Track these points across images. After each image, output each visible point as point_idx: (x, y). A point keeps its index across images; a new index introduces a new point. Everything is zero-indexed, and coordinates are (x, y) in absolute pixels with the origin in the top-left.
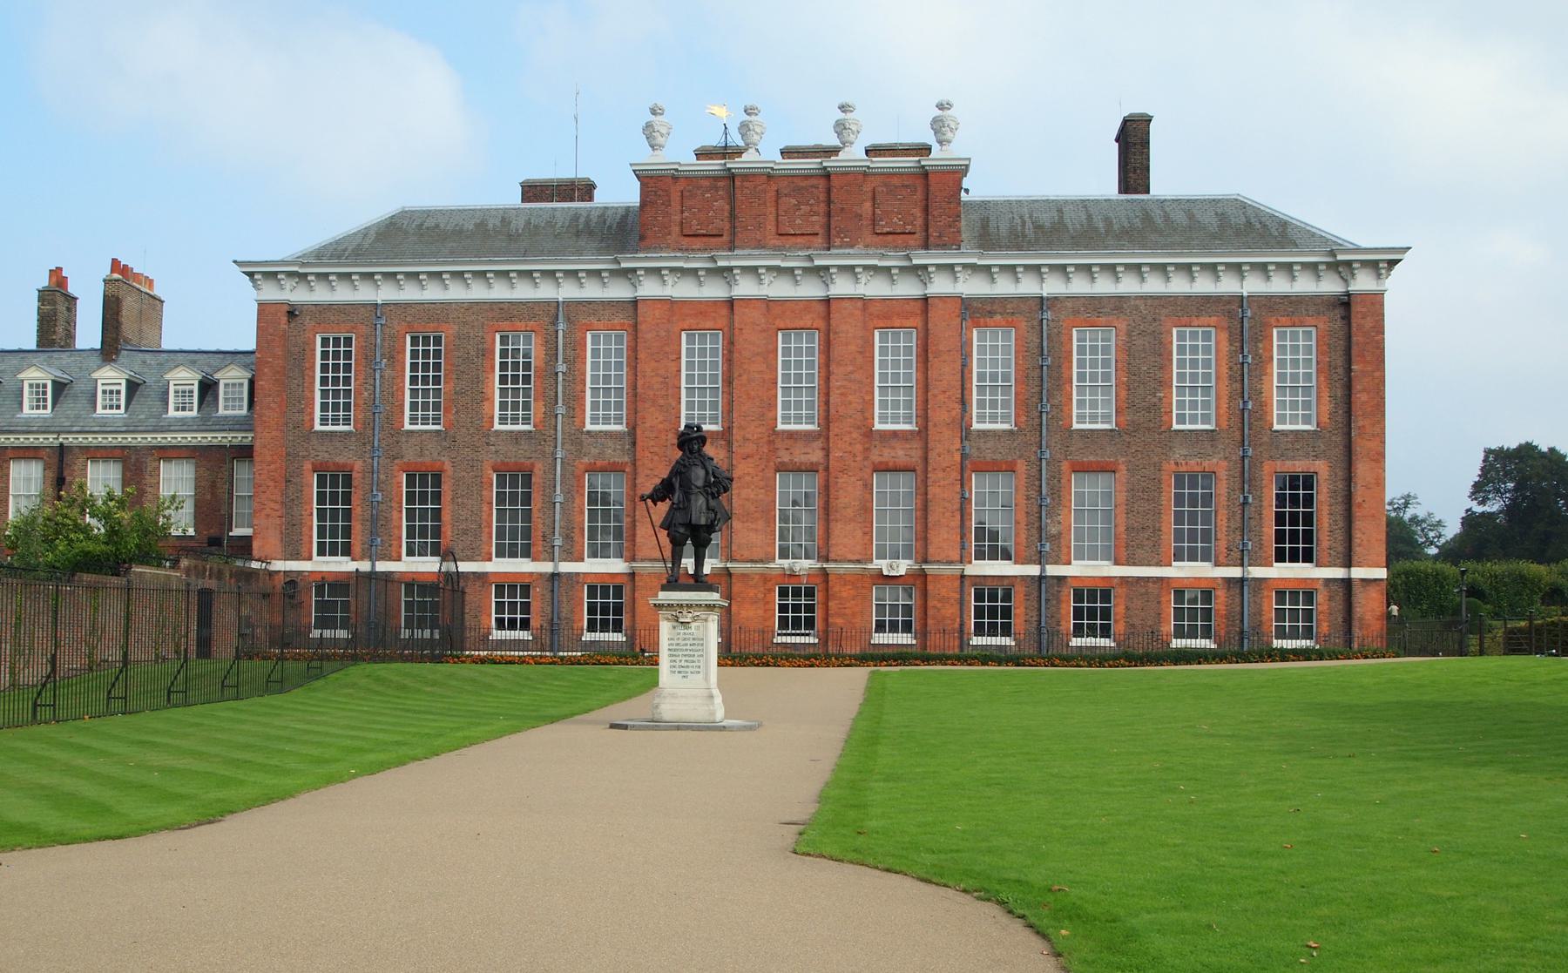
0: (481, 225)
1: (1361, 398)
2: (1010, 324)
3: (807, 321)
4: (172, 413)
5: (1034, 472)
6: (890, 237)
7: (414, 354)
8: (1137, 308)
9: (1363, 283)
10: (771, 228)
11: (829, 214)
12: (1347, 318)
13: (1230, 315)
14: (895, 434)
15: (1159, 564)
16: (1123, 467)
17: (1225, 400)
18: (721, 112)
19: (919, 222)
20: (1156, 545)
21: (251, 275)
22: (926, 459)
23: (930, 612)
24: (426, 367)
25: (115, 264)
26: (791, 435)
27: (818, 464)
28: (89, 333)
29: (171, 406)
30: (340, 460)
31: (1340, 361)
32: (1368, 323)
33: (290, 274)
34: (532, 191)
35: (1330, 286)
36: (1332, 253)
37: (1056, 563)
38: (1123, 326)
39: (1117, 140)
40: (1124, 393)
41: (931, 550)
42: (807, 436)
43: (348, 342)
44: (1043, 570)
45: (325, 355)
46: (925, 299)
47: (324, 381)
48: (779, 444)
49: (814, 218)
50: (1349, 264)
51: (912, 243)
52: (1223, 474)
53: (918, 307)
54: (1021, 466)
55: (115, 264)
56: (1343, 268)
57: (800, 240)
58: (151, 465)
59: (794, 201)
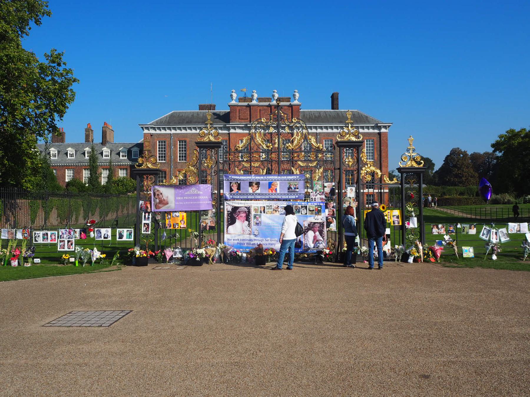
0: (193, 115)
1: (383, 154)
4: (121, 158)
7: (180, 145)
9: (383, 130)
12: (380, 138)
18: (245, 90)
21: (142, 128)
24: (182, 148)
25: (105, 124)
28: (97, 138)
29: (121, 156)
30: (163, 169)
32: (385, 138)
33: (151, 128)
34: (202, 107)
35: (376, 131)
36: (377, 124)
43: (165, 142)
45: (159, 145)
47: (159, 151)
55: (105, 124)
56: (379, 128)
58: (117, 169)
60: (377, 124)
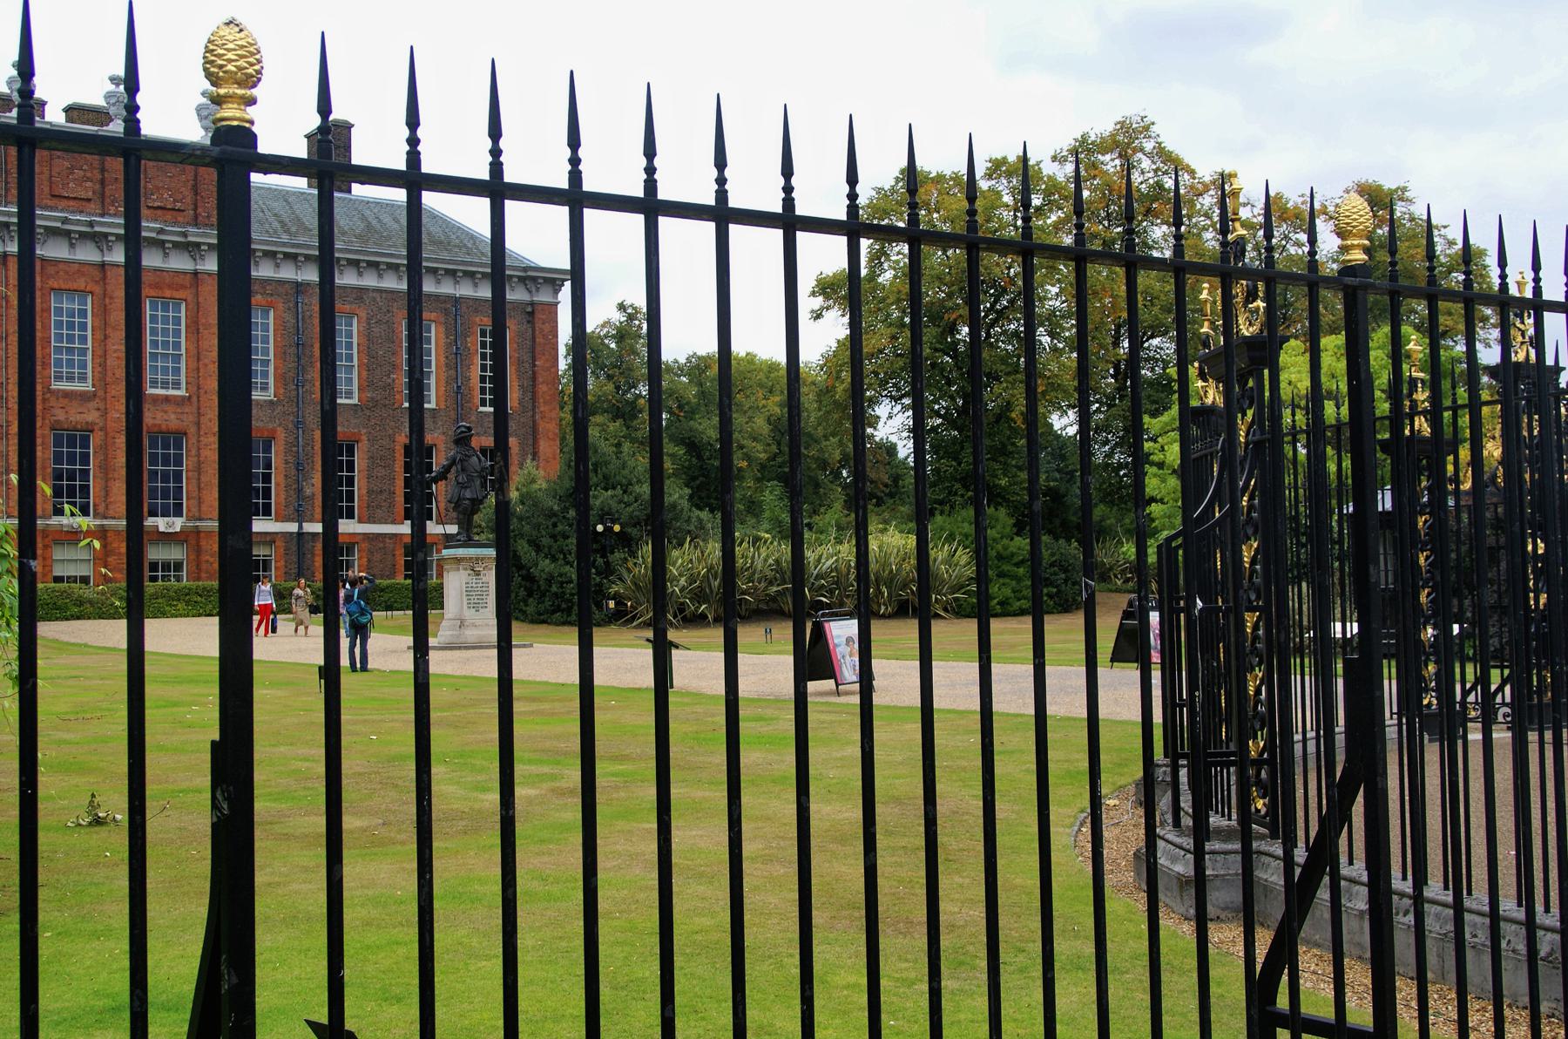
2: (271, 305)
3: (81, 283)
5: (291, 439)
6: (159, 212)
8: (374, 299)
9: (543, 297)
10: (46, 190)
11: (103, 182)
13: (446, 312)
14: (167, 399)
15: (393, 522)
16: (364, 438)
17: (443, 383)
19: (189, 200)
20: (392, 505)
22: (198, 424)
23: (204, 566)
26: (67, 395)
27: (93, 424)
31: (527, 357)
32: (547, 327)
37: (311, 521)
38: (363, 314)
39: (308, 137)
40: (365, 373)
41: (204, 508)
42: (84, 397)
44: (300, 527)
46: (196, 273)
48: (53, 402)
49: (89, 184)
50: (534, 279)
51: (181, 219)
52: (442, 447)
53: (188, 280)
54: (281, 434)
57: (71, 203)
59: (67, 164)
60: (526, 269)
